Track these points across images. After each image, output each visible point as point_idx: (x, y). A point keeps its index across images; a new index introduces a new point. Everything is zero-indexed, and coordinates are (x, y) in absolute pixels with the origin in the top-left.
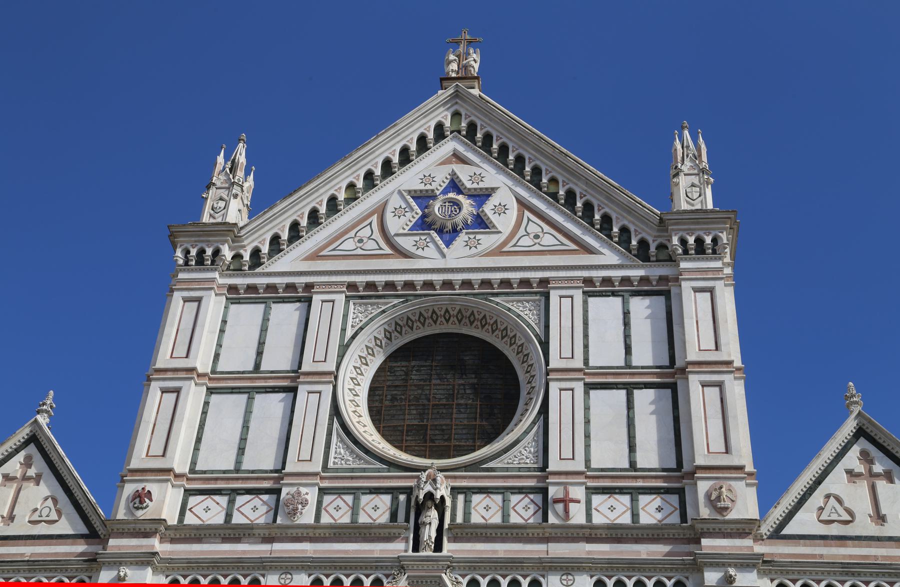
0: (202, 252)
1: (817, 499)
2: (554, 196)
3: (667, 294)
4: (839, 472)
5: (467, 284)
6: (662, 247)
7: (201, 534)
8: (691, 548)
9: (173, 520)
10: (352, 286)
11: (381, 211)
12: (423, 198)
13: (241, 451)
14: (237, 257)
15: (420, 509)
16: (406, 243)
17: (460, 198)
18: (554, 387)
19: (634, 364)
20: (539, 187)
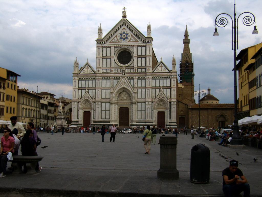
0: (99, 43)
1: (157, 69)
2: (135, 34)
3: (145, 47)
4: (159, 66)
5: (126, 46)
6: (145, 41)
7: (104, 73)
8: (146, 74)
9: (101, 72)
10: (115, 46)
11: (116, 36)
12: (121, 34)
13: (106, 65)
14: (103, 43)
15: (123, 71)
16: (120, 41)
17: (125, 35)
18: (135, 58)
19: (142, 55)
20: (133, 33)
